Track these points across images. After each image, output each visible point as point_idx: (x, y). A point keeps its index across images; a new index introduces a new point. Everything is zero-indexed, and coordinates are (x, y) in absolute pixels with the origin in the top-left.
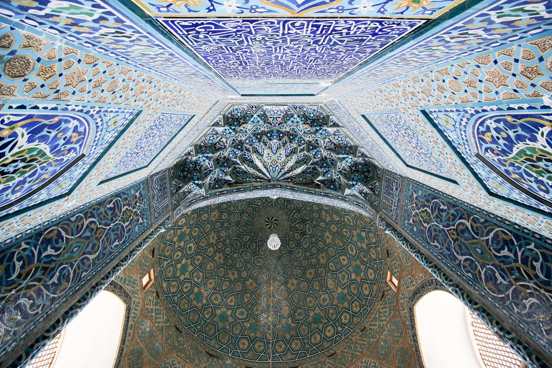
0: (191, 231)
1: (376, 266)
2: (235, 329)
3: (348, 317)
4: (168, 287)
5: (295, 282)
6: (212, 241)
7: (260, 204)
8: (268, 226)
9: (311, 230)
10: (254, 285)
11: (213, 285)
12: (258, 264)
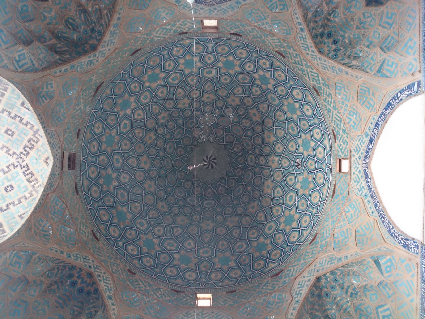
0: (230, 75)
1: (204, 280)
2: (113, 117)
3: (135, 253)
4: (183, 46)
5: (152, 190)
6: (206, 95)
7: (235, 149)
8: (205, 158)
9: (208, 206)
10: (149, 142)
11: (160, 95)
12: (168, 146)
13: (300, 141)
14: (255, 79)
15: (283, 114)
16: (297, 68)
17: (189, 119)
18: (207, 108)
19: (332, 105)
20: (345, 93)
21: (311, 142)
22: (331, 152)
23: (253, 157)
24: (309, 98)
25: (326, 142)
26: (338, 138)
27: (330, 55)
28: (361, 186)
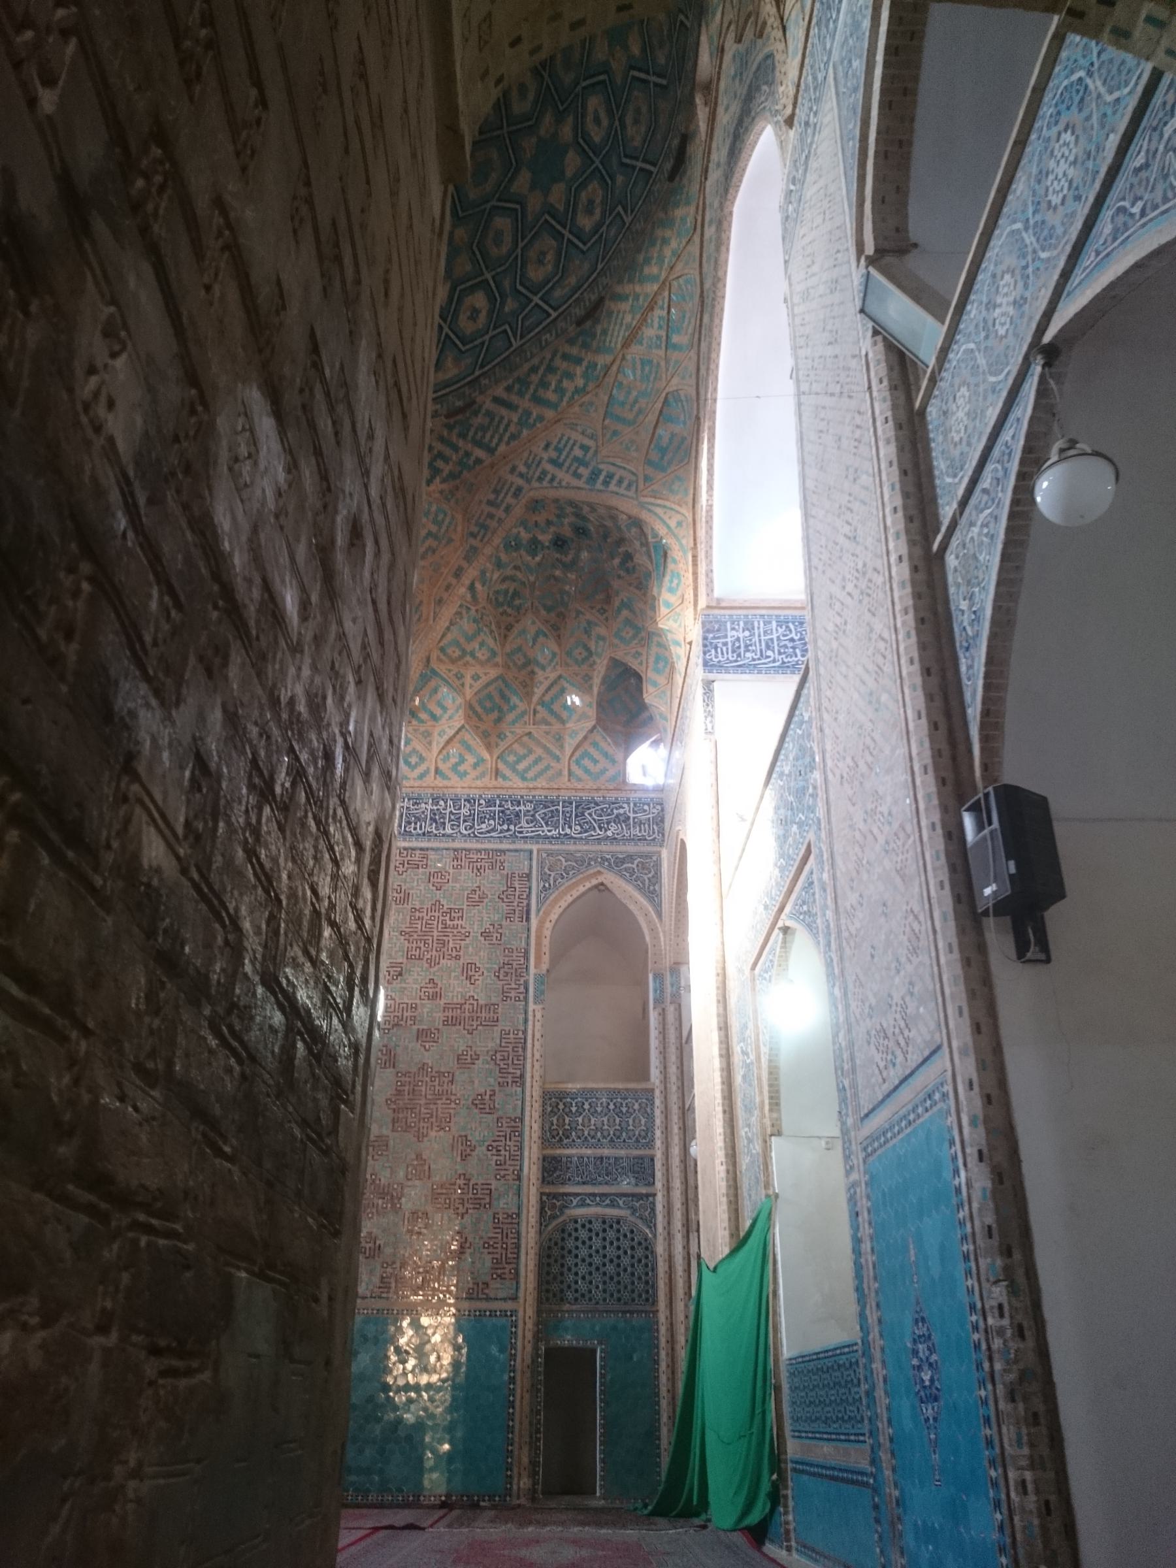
16: (535, 361)
27: (521, 529)
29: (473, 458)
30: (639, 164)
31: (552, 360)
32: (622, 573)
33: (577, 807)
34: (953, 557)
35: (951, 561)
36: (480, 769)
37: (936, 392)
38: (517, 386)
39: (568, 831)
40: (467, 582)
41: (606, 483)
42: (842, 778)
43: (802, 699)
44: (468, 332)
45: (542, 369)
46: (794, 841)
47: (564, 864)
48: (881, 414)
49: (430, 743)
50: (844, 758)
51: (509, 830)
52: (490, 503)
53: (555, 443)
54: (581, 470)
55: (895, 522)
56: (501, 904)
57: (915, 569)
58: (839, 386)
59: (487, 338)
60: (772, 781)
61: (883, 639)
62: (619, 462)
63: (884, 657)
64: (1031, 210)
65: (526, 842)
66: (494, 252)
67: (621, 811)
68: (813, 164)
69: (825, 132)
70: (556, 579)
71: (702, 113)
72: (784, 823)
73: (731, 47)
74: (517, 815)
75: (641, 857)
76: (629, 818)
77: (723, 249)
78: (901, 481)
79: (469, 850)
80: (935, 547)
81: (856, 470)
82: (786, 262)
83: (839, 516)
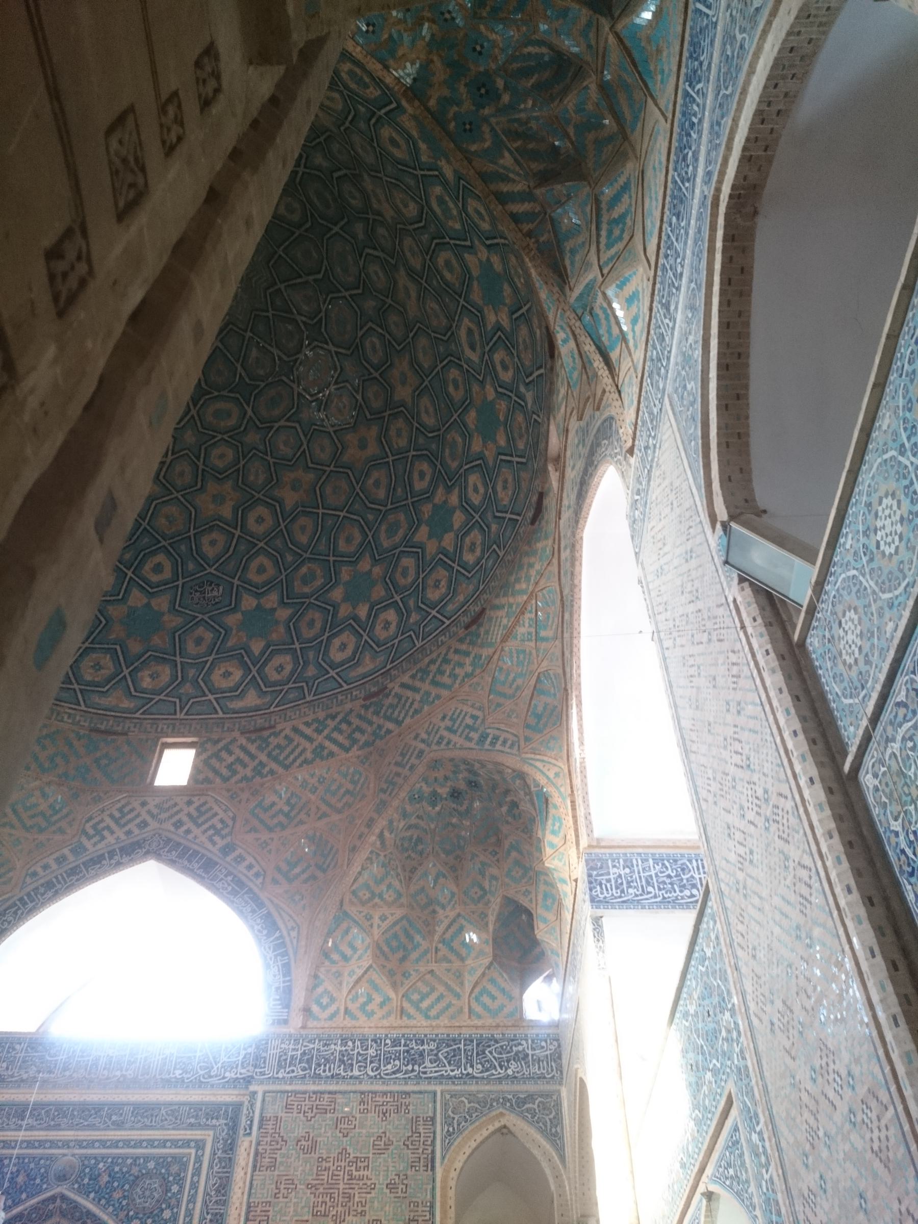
7: (254, 353)
13: (272, 600)
14: (449, 489)
15: (352, 549)
17: (336, 194)
18: (381, 274)
19: (327, 743)
20: (343, 790)
21: (262, 644)
22: (221, 715)
23: (232, 422)
24: (368, 665)
25: (252, 699)
26: (253, 742)
27: (423, 784)
28: (106, 833)
29: (384, 730)
30: (508, 516)
31: (446, 654)
32: (510, 819)
33: (478, 1045)
34: (869, 776)
35: (868, 780)
36: (386, 1009)
37: (815, 624)
38: (419, 675)
39: (470, 1070)
40: (377, 831)
41: (493, 744)
42: (772, 1024)
43: (701, 934)
44: (382, 638)
45: (440, 660)
46: (710, 1090)
47: (468, 1105)
48: (760, 647)
49: (341, 983)
50: (772, 1002)
51: (413, 1070)
52: (397, 764)
53: (450, 714)
54: (472, 734)
55: (797, 745)
56: (406, 1151)
57: (830, 791)
58: (706, 634)
59: (396, 641)
60: (676, 1020)
61: (804, 867)
62: (502, 727)
63: (810, 887)
64: (904, 436)
65: (429, 1083)
66: (402, 582)
67: (520, 1048)
68: (656, 473)
69: (665, 446)
70: (454, 826)
71: (554, 476)
72: (694, 1068)
73: (574, 425)
74: (421, 1054)
75: (541, 1096)
76: (527, 1055)
77: (577, 563)
78: (794, 706)
79: (375, 1093)
80: (847, 767)
81: (739, 704)
82: (636, 553)
83: (725, 748)
